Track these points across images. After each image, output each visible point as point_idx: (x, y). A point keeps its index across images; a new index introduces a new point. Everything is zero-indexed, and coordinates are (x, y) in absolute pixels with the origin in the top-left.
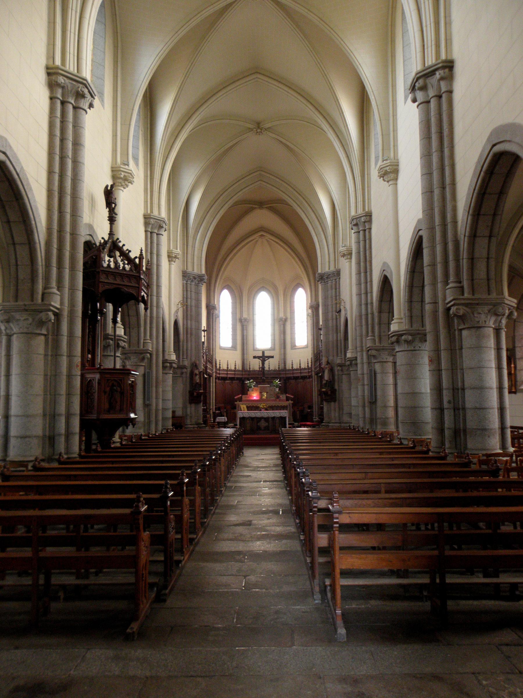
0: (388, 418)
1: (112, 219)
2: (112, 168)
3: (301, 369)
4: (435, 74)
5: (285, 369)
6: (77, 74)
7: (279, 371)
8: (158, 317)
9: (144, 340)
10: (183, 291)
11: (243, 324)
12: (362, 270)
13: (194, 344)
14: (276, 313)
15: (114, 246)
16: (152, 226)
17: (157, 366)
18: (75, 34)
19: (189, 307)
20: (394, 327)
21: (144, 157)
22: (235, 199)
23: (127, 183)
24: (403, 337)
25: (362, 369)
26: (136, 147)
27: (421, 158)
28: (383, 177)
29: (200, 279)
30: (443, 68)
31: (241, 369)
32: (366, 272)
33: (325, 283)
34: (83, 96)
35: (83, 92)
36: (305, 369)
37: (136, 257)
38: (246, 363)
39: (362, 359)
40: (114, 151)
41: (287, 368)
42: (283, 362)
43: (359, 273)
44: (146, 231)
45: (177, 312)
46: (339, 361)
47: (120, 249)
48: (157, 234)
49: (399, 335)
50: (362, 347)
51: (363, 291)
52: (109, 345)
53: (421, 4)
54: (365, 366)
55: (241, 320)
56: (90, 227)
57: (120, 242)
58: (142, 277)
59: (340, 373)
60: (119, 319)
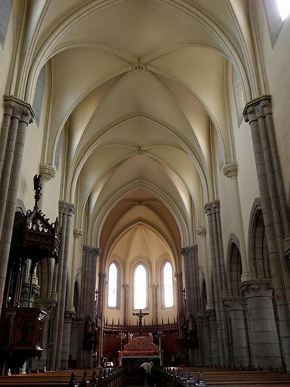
0: (243, 357)
1: (37, 197)
2: (40, 166)
3: (169, 325)
4: (260, 104)
6: (24, 101)
8: (64, 275)
9: (52, 292)
10: (83, 261)
11: (125, 290)
12: (215, 241)
13: (89, 301)
14: (150, 281)
15: (37, 216)
16: (65, 209)
17: (61, 313)
18: (25, 80)
19: (87, 272)
20: (244, 279)
21: (62, 164)
22: (122, 197)
23: (49, 176)
24: (251, 286)
25: (220, 316)
26: (57, 157)
27: (255, 155)
28: (227, 174)
29: (95, 252)
30: (265, 100)
31: (123, 324)
32: (218, 242)
33: (185, 255)
34: (27, 115)
35: (27, 112)
36: (172, 324)
37: (53, 224)
39: (219, 308)
40: (43, 155)
41: (159, 324)
42: (155, 319)
43: (213, 243)
44: (59, 213)
45: (77, 275)
46: (199, 314)
47: (42, 219)
48: (67, 215)
49: (248, 285)
50: (218, 299)
51: (217, 256)
52: (26, 292)
53: (246, 66)
54: (222, 314)
55: (124, 286)
56: (21, 202)
57: (42, 213)
58: (56, 237)
59: (201, 324)
60: (35, 271)
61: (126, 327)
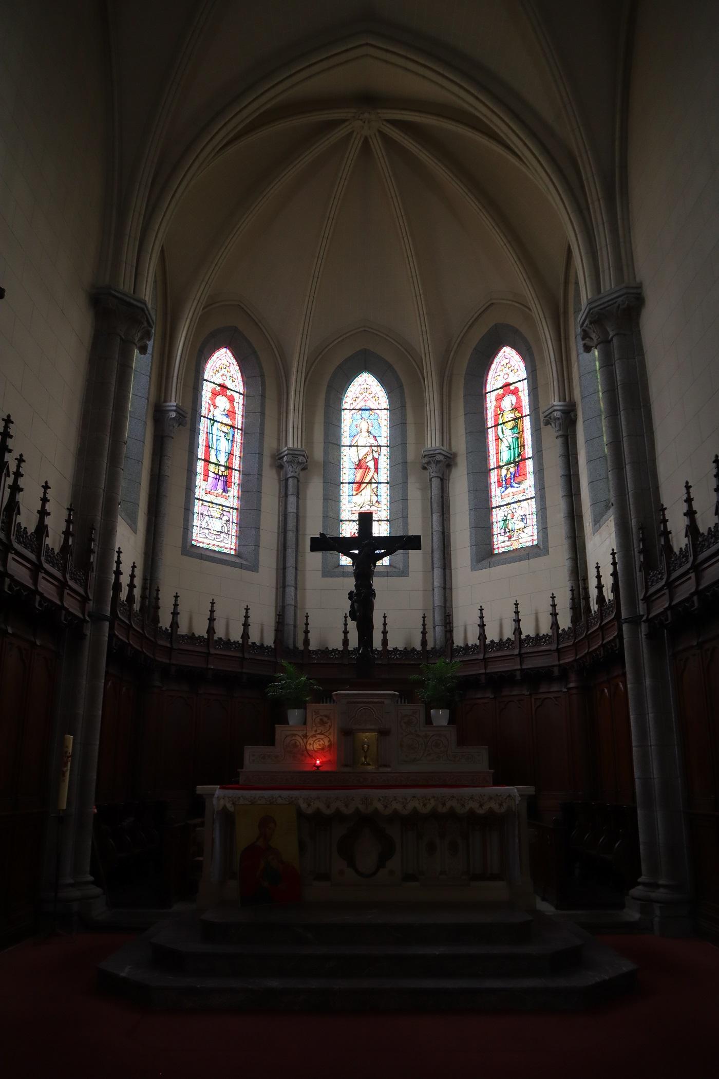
3: (519, 641)
5: (448, 648)
7: (426, 654)
11: (290, 465)
31: (269, 641)
38: (289, 619)
41: (458, 641)
42: (438, 618)
55: (278, 463)
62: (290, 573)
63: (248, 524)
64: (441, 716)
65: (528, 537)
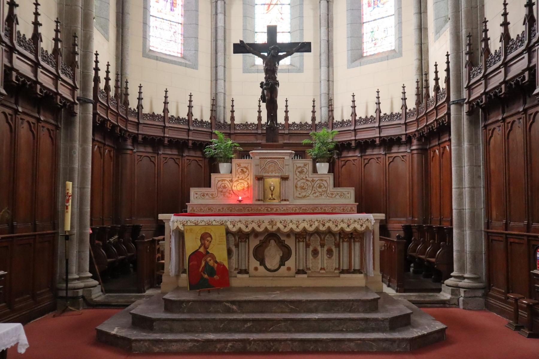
5: (330, 123)
7: (315, 126)
31: (207, 118)
38: (220, 103)
41: (337, 118)
42: (324, 102)
61: (221, 126)
62: (220, 70)
63: (190, 35)
64: (323, 167)
65: (388, 43)
